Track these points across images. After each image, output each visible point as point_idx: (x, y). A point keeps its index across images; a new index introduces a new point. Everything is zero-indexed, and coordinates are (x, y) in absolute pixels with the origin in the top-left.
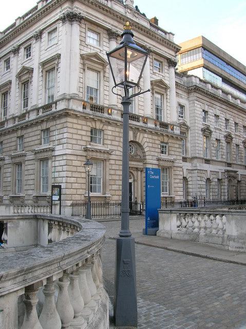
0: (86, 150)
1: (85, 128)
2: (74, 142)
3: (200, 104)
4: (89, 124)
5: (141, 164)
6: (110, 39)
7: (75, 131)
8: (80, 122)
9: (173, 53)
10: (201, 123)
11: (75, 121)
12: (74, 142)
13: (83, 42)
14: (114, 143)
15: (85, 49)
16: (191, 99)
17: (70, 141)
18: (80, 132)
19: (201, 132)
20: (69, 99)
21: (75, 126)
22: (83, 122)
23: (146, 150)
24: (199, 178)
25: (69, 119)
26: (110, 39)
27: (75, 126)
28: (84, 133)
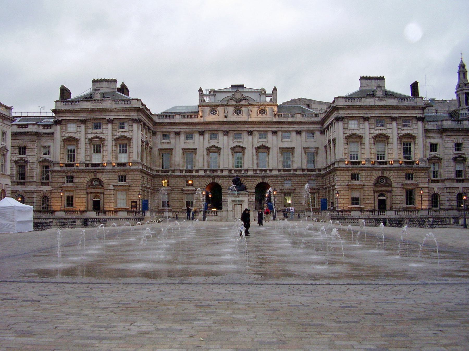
0: (348, 185)
1: (347, 174)
2: (341, 182)
3: (451, 139)
4: (350, 172)
5: (390, 188)
6: (364, 121)
7: (341, 177)
8: (344, 172)
9: (420, 111)
10: (453, 153)
11: (342, 172)
12: (341, 182)
13: (345, 128)
14: (367, 179)
15: (348, 132)
16: (443, 137)
17: (339, 182)
18: (344, 177)
19: (452, 161)
20: (339, 161)
21: (342, 174)
22: (347, 172)
23: (392, 180)
24: (448, 194)
25: (339, 172)
26: (364, 121)
27: (342, 174)
28: (347, 177)
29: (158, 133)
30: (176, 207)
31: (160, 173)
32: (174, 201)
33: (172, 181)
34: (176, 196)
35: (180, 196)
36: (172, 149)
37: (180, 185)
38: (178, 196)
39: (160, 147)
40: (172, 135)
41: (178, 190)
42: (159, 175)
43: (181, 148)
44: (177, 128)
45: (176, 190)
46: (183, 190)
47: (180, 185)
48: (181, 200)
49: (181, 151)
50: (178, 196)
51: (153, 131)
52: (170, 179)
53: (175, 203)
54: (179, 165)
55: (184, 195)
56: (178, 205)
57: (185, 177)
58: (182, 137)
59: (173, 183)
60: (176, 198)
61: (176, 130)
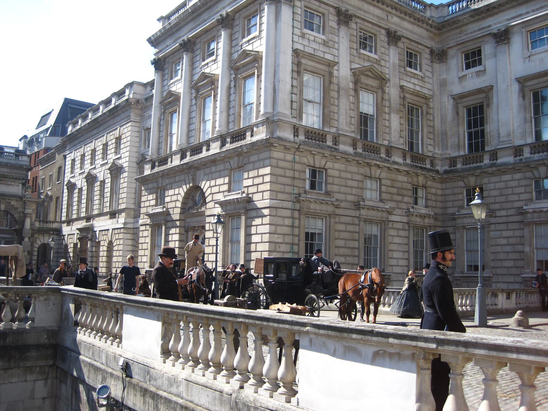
29: (451, 52)
30: (505, 271)
31: (459, 166)
32: (499, 249)
33: (492, 186)
34: (505, 234)
35: (518, 233)
36: (491, 88)
37: (516, 198)
38: (510, 233)
39: (457, 89)
40: (487, 49)
41: (512, 212)
42: (456, 171)
43: (513, 78)
44: (496, 23)
45: (503, 213)
46: (522, 212)
47: (516, 198)
48: (519, 248)
49: (516, 87)
50: (510, 233)
51: (432, 52)
52: (485, 180)
53: (501, 256)
54: (509, 135)
55: (526, 230)
56: (511, 264)
57: (528, 166)
58: (517, 42)
59: (493, 193)
60: (504, 241)
61: (495, 29)
